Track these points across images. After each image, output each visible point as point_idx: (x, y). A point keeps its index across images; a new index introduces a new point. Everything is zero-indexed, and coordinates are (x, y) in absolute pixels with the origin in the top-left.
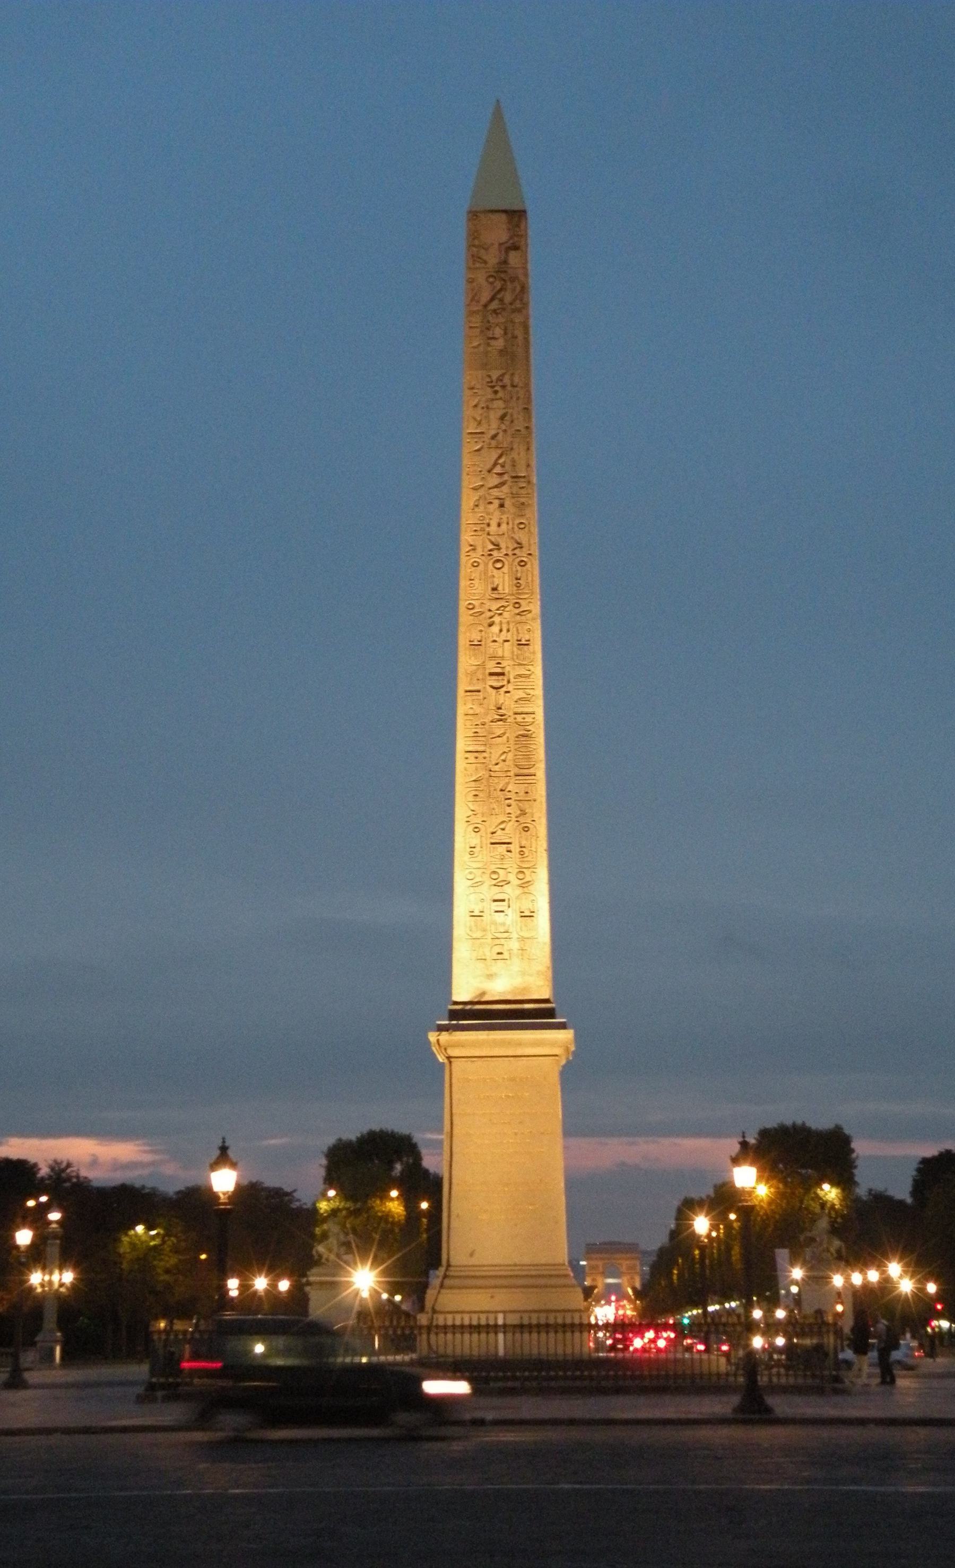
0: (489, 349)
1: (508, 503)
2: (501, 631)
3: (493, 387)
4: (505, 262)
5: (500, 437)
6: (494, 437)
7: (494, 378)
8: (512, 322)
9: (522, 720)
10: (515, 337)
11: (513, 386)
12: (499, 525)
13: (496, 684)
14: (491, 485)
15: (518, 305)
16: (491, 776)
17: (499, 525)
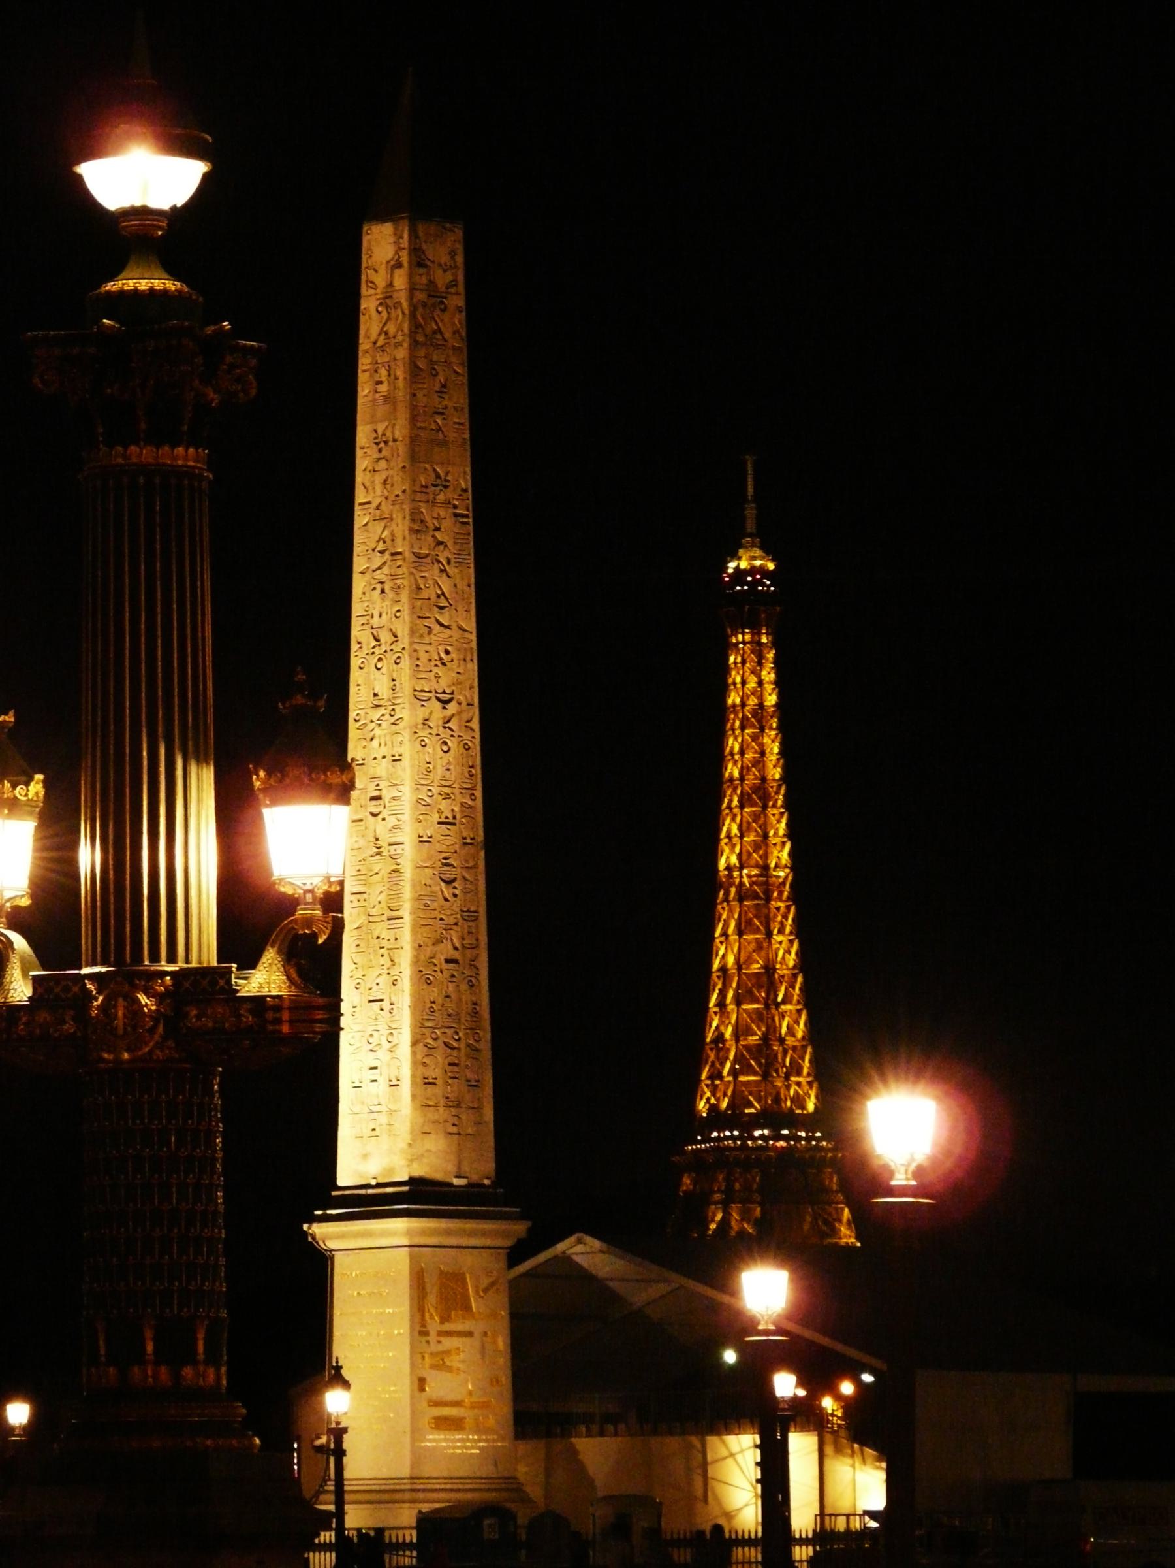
0: (377, 395)
1: (387, 588)
2: (380, 745)
3: (377, 444)
4: (391, 285)
5: (383, 507)
6: (378, 508)
7: (380, 433)
8: (395, 359)
9: (395, 853)
10: (396, 378)
11: (395, 440)
12: (380, 616)
13: (375, 811)
14: (375, 567)
15: (400, 338)
16: (370, 922)
17: (380, 616)
